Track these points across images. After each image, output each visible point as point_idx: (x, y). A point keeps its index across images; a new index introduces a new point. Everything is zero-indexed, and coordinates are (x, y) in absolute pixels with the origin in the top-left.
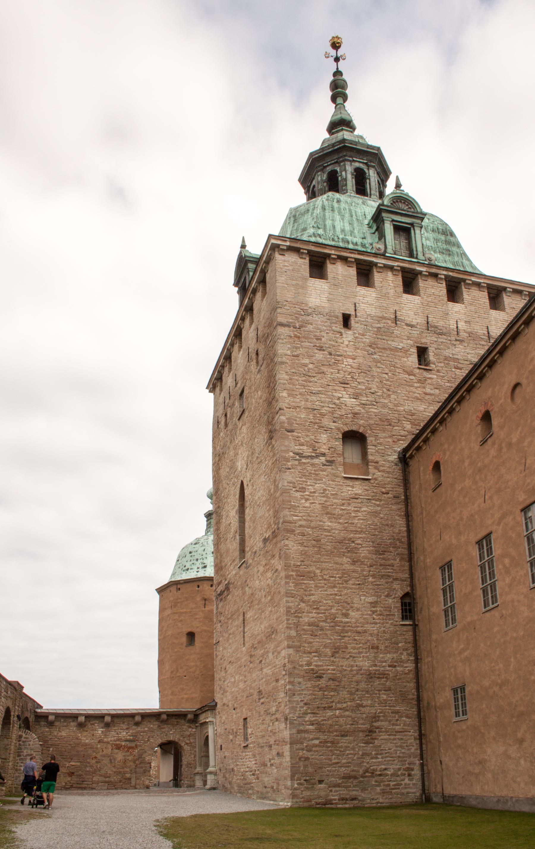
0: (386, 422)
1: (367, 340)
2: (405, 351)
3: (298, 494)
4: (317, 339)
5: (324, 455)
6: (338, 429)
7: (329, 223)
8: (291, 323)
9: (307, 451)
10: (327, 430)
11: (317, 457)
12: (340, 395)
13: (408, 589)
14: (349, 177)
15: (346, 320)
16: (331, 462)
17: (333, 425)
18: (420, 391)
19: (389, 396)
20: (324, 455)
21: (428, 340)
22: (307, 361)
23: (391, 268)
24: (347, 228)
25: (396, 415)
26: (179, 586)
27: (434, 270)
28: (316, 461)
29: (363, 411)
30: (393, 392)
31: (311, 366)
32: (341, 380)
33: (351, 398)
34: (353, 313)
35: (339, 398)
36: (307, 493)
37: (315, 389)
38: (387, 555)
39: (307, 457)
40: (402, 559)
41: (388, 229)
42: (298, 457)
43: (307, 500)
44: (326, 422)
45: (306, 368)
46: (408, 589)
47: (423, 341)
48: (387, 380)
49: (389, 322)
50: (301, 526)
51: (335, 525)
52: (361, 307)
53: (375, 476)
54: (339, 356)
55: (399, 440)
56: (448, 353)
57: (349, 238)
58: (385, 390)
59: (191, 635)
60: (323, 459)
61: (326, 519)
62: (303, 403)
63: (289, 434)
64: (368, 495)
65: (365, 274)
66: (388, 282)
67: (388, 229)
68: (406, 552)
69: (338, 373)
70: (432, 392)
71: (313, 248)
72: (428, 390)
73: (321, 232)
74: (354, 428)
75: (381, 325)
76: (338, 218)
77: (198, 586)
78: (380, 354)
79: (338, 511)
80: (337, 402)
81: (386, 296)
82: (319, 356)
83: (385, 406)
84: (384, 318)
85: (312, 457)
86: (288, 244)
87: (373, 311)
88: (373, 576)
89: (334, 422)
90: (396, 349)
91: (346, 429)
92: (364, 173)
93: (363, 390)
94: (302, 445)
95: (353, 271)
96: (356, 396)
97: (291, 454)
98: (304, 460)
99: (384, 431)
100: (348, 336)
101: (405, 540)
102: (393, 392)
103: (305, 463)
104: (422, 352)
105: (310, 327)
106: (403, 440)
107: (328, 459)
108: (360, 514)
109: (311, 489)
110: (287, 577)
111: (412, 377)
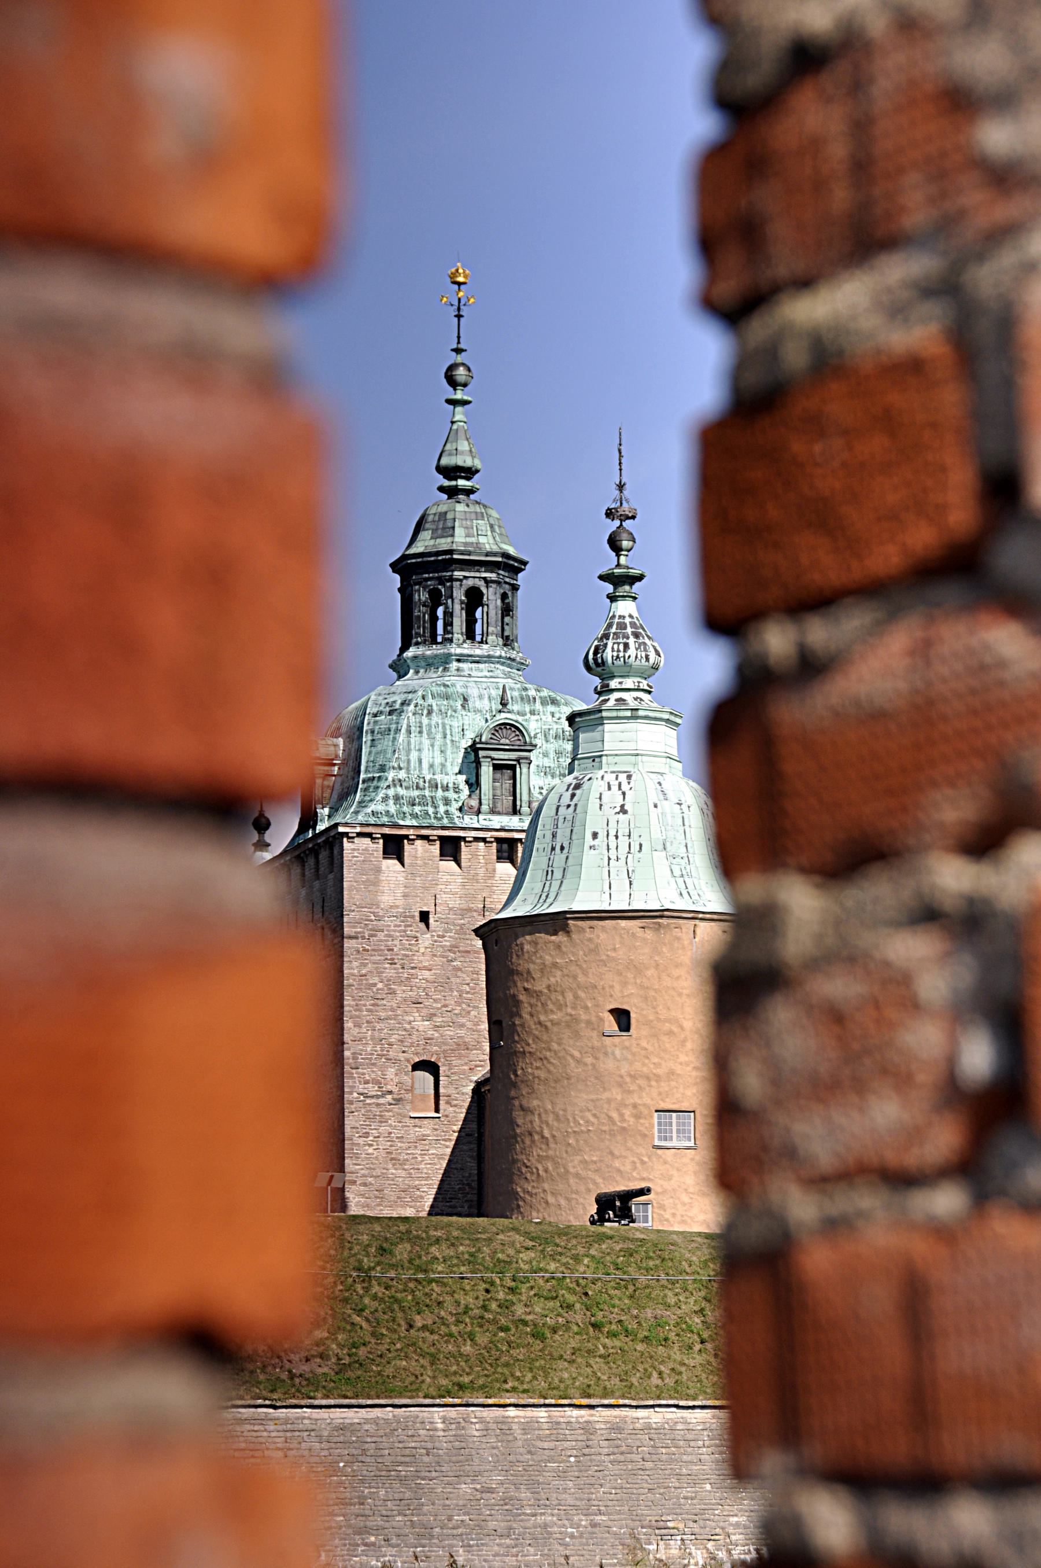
3: (361, 1141)
4: (389, 950)
5: (390, 1092)
6: (408, 1061)
8: (359, 933)
9: (372, 1089)
10: (396, 1061)
11: (383, 1096)
12: (412, 1019)
14: (457, 607)
15: (424, 917)
16: (398, 1101)
19: (469, 1012)
20: (390, 1092)
22: (376, 980)
25: (476, 1037)
28: (382, 1101)
29: (436, 1035)
30: (474, 1007)
31: (380, 985)
32: (413, 1000)
33: (423, 1020)
34: (432, 909)
35: (410, 1023)
36: (371, 1138)
37: (383, 1015)
38: (454, 1202)
39: (372, 1097)
41: (486, 771)
42: (362, 1098)
43: (371, 1145)
45: (375, 989)
48: (468, 993)
49: (475, 914)
50: (364, 1176)
51: (401, 1173)
52: (442, 898)
53: (446, 1113)
54: (413, 968)
55: (477, 1066)
57: (439, 778)
58: (464, 1006)
60: (389, 1097)
62: (370, 1033)
63: (354, 1071)
64: (437, 1136)
65: (451, 848)
66: (478, 856)
68: (475, 1198)
69: (411, 990)
73: (402, 775)
74: (425, 1058)
76: (426, 742)
78: (462, 959)
80: (408, 1026)
81: (475, 879)
82: (390, 972)
84: (470, 910)
85: (378, 1097)
87: (455, 903)
89: (404, 1052)
92: (482, 594)
93: (438, 1009)
94: (367, 1082)
95: (436, 848)
96: (430, 1017)
97: (355, 1095)
98: (368, 1101)
99: (460, 1057)
100: (426, 939)
101: (475, 1184)
102: (474, 1007)
103: (369, 1104)
105: (381, 936)
106: (481, 1066)
107: (395, 1096)
108: (427, 1157)
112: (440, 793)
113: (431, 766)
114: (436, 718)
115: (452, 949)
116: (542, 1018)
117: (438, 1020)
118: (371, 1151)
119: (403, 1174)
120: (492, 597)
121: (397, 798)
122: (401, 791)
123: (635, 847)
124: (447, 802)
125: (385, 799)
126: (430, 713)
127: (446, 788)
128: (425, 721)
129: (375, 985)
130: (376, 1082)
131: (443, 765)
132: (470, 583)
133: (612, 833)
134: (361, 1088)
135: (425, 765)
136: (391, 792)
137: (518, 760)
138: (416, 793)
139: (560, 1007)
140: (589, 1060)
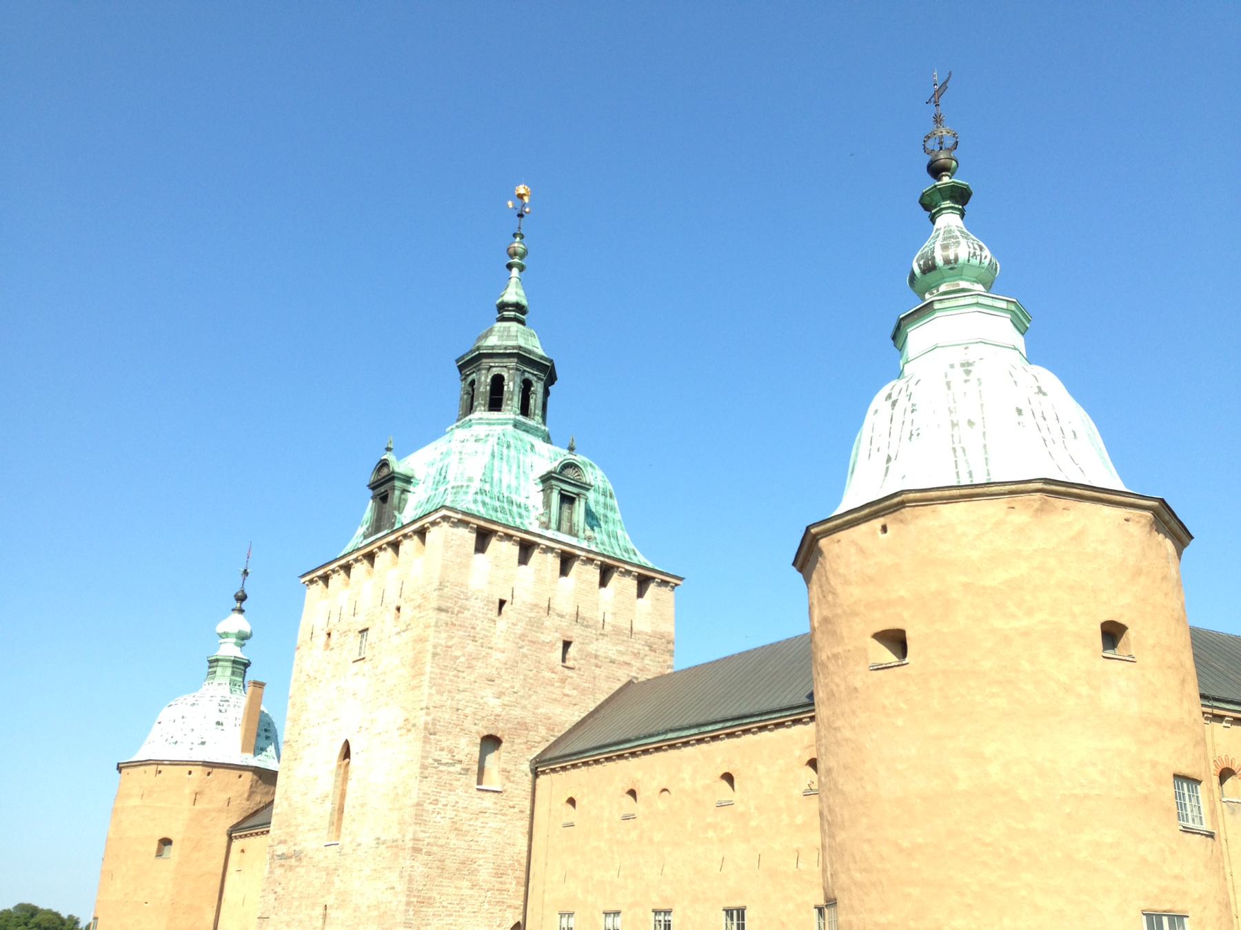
0: (523, 726)
1: (519, 630)
2: (552, 645)
5: (460, 762)
7: (496, 476)
9: (445, 757)
11: (452, 765)
13: (520, 918)
15: (502, 603)
17: (474, 729)
18: (558, 691)
20: (460, 762)
21: (575, 633)
23: (552, 550)
24: (514, 483)
26: (160, 768)
27: (591, 556)
28: (451, 769)
37: (462, 687)
38: (504, 879)
40: (518, 883)
44: (468, 724)
46: (520, 918)
47: (569, 634)
56: (592, 648)
57: (514, 497)
59: (166, 842)
60: (458, 767)
61: (452, 836)
65: (526, 549)
67: (555, 498)
68: (523, 875)
70: (570, 693)
71: (482, 523)
72: (566, 691)
73: (487, 487)
75: (532, 615)
76: (505, 468)
77: (190, 773)
79: (465, 828)
82: (471, 647)
83: (524, 707)
84: (536, 605)
86: (460, 516)
88: (489, 902)
90: (544, 643)
91: (486, 733)
94: (442, 750)
96: (500, 695)
97: (430, 761)
99: (519, 736)
100: (502, 623)
104: (567, 644)
105: (467, 614)
109: (443, 801)
110: (408, 904)
111: (553, 675)
112: (515, 509)
113: (509, 487)
114: (513, 452)
115: (522, 637)
116: (999, 624)
117: (506, 699)
118: (438, 819)
119: (464, 845)
120: (538, 387)
121: (484, 504)
122: (487, 500)
123: (1069, 434)
124: (521, 516)
125: (475, 501)
126: (508, 447)
127: (519, 506)
128: (505, 451)
129: (457, 658)
130: (451, 751)
131: (517, 489)
132: (527, 375)
133: (1039, 415)
134: (437, 755)
135: (504, 485)
136: (479, 497)
137: (578, 495)
138: (497, 504)
139: (1030, 612)
140: (1084, 690)
